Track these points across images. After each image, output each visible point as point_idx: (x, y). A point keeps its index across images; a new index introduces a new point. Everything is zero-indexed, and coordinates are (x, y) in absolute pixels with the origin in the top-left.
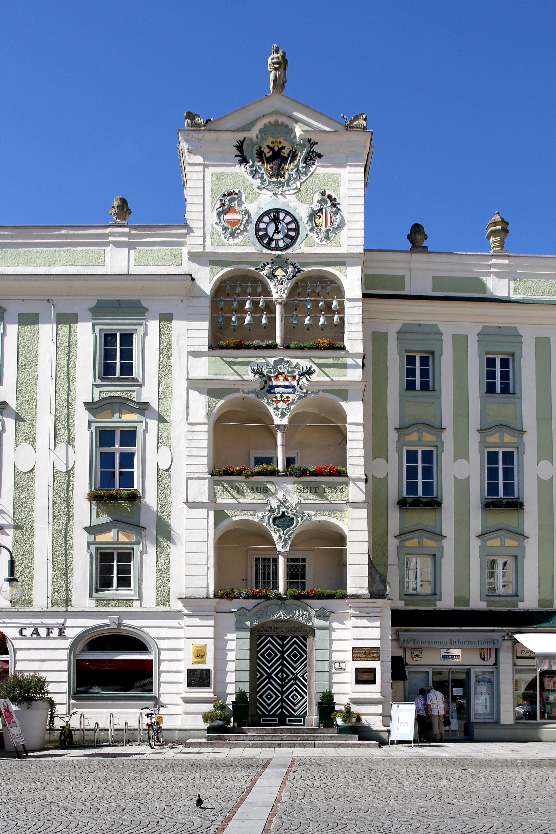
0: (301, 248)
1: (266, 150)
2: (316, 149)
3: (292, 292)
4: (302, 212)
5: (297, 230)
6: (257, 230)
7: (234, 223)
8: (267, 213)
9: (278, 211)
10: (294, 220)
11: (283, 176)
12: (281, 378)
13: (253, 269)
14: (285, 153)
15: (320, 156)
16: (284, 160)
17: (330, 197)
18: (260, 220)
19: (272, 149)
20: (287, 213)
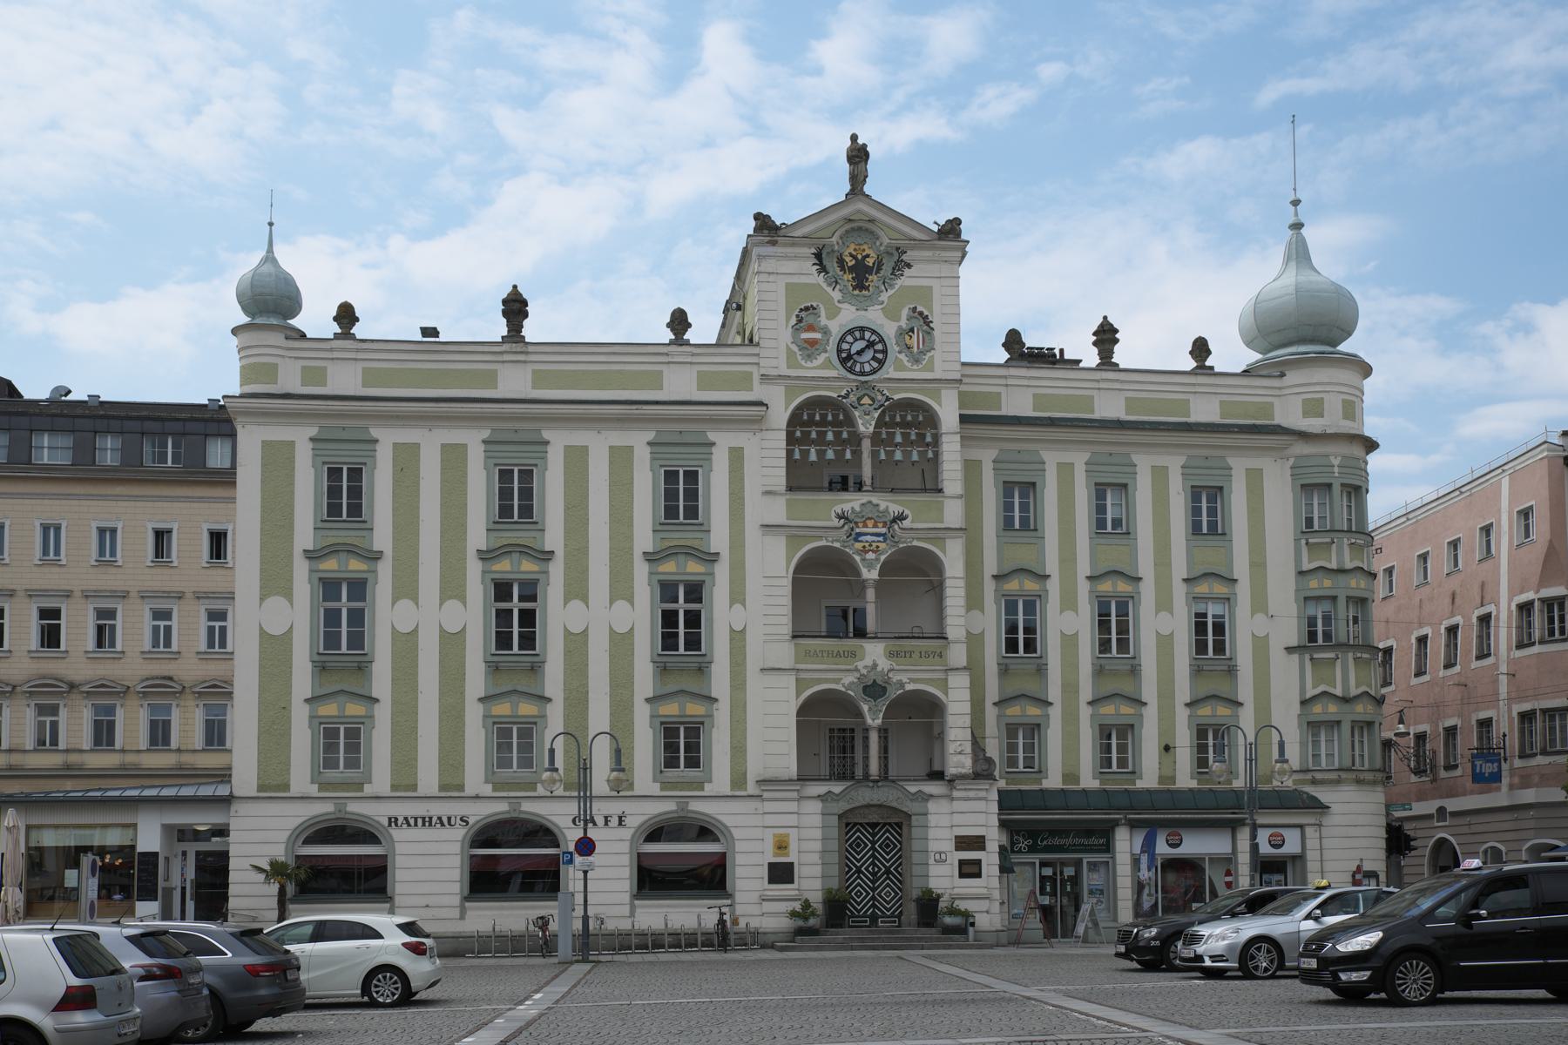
0: (889, 371)
1: (848, 259)
2: (904, 257)
3: (880, 423)
4: (889, 330)
5: (885, 352)
6: (839, 351)
7: (812, 343)
8: (850, 332)
9: (862, 329)
10: (882, 340)
11: (867, 288)
12: (870, 523)
13: (835, 395)
14: (870, 262)
15: (909, 266)
16: (869, 270)
17: (921, 313)
18: (842, 340)
19: (854, 257)
20: (874, 332)
